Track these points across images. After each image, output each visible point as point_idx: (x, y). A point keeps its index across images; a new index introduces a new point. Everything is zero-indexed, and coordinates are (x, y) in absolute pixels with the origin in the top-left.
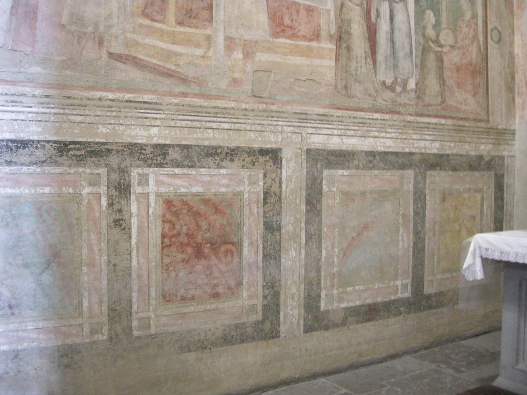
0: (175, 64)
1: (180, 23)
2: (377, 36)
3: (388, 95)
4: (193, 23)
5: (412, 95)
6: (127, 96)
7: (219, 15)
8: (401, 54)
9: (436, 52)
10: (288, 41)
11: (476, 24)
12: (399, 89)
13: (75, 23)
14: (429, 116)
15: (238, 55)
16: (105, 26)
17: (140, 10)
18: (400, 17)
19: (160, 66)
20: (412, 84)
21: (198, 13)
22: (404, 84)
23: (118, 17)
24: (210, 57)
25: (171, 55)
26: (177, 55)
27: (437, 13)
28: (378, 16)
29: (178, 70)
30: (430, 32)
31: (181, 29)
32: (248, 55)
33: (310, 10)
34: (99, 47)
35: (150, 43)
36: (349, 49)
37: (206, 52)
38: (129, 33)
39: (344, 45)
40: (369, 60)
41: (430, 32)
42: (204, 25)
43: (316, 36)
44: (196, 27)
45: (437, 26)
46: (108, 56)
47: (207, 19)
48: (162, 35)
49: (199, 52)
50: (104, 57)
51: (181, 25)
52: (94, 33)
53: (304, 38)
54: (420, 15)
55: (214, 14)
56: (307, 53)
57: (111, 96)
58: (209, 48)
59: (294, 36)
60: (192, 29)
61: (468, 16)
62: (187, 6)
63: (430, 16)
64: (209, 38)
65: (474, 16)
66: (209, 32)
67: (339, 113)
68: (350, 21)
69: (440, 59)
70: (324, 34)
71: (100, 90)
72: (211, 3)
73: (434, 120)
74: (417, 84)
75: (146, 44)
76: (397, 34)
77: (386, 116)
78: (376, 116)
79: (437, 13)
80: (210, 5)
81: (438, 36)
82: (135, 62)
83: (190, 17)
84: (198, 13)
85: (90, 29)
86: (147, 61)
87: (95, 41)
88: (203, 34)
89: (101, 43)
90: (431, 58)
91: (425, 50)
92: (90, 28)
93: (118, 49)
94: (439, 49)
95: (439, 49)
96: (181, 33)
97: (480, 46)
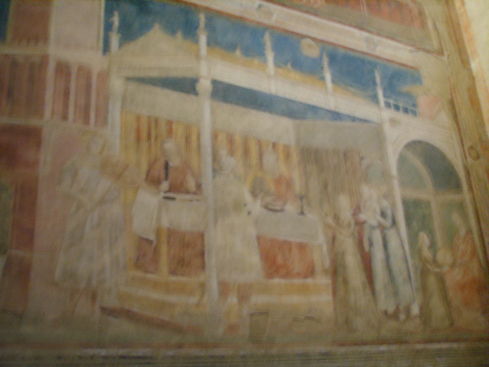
1: (173, 272)
2: (373, 265)
3: (392, 324)
5: (418, 321)
6: (121, 352)
7: (212, 261)
8: (400, 279)
9: (436, 274)
10: (283, 281)
11: (472, 239)
12: (402, 317)
14: (439, 341)
15: (233, 300)
18: (393, 243)
20: (415, 310)
22: (408, 310)
27: (431, 234)
28: (371, 244)
30: (427, 253)
31: (174, 278)
32: (243, 297)
33: (302, 247)
36: (346, 282)
39: (340, 279)
40: (368, 291)
41: (427, 253)
43: (311, 272)
45: (433, 246)
48: (156, 285)
49: (193, 300)
53: (299, 275)
54: (413, 238)
56: (304, 290)
57: (103, 352)
58: (203, 294)
59: (288, 275)
61: (463, 232)
63: (424, 239)
64: (203, 286)
65: (469, 231)
66: (202, 278)
67: (343, 350)
68: (343, 254)
69: (441, 280)
70: (318, 268)
71: (91, 347)
73: (445, 346)
74: (421, 309)
76: (393, 260)
77: (394, 348)
78: (383, 348)
79: (431, 234)
81: (435, 256)
82: (129, 315)
85: (83, 285)
89: (94, 297)
90: (432, 281)
91: (424, 273)
93: (111, 302)
94: (437, 270)
95: (437, 270)
97: (480, 261)
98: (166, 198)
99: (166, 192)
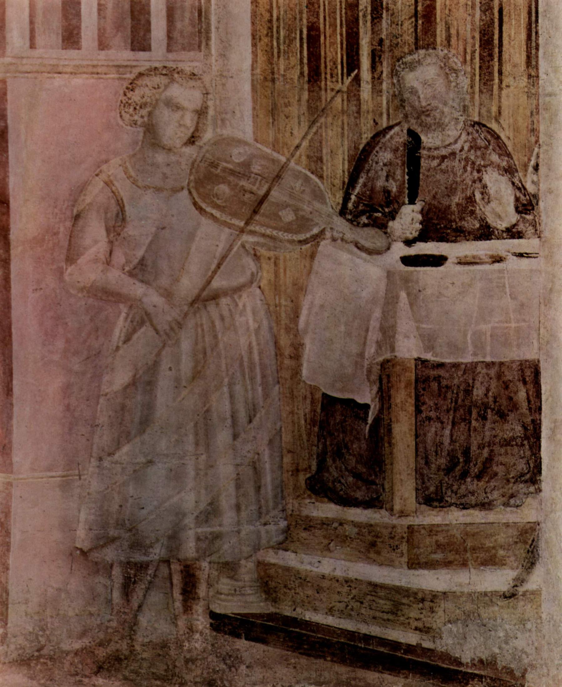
0: (416, 629)
4: (473, 493)
13: (113, 540)
16: (198, 539)
17: (302, 478)
19: (367, 638)
21: (489, 460)
23: (238, 508)
24: (533, 593)
25: (405, 601)
26: (423, 600)
29: (427, 644)
34: (185, 601)
35: (339, 573)
37: (519, 581)
38: (271, 551)
42: (512, 496)
44: (485, 506)
46: (211, 625)
47: (522, 475)
50: (200, 627)
51: (436, 504)
52: (167, 562)
55: (544, 453)
60: (471, 511)
62: (452, 441)
72: (533, 421)
75: (323, 577)
80: (531, 427)
83: (464, 475)
84: (489, 460)
86: (328, 629)
87: (172, 584)
88: (507, 525)
92: (157, 551)
96: (432, 530)
98: (407, 261)
99: (409, 243)
